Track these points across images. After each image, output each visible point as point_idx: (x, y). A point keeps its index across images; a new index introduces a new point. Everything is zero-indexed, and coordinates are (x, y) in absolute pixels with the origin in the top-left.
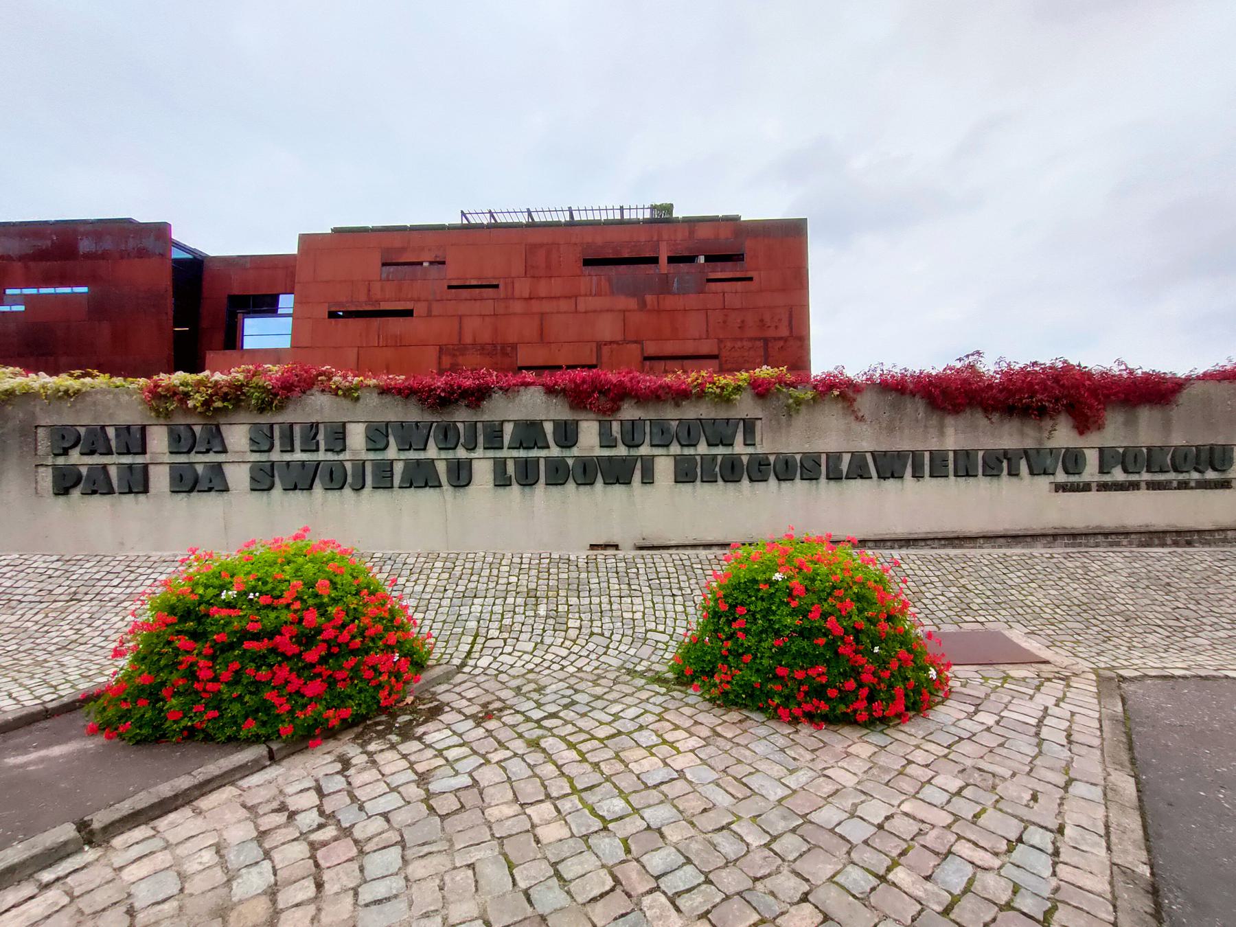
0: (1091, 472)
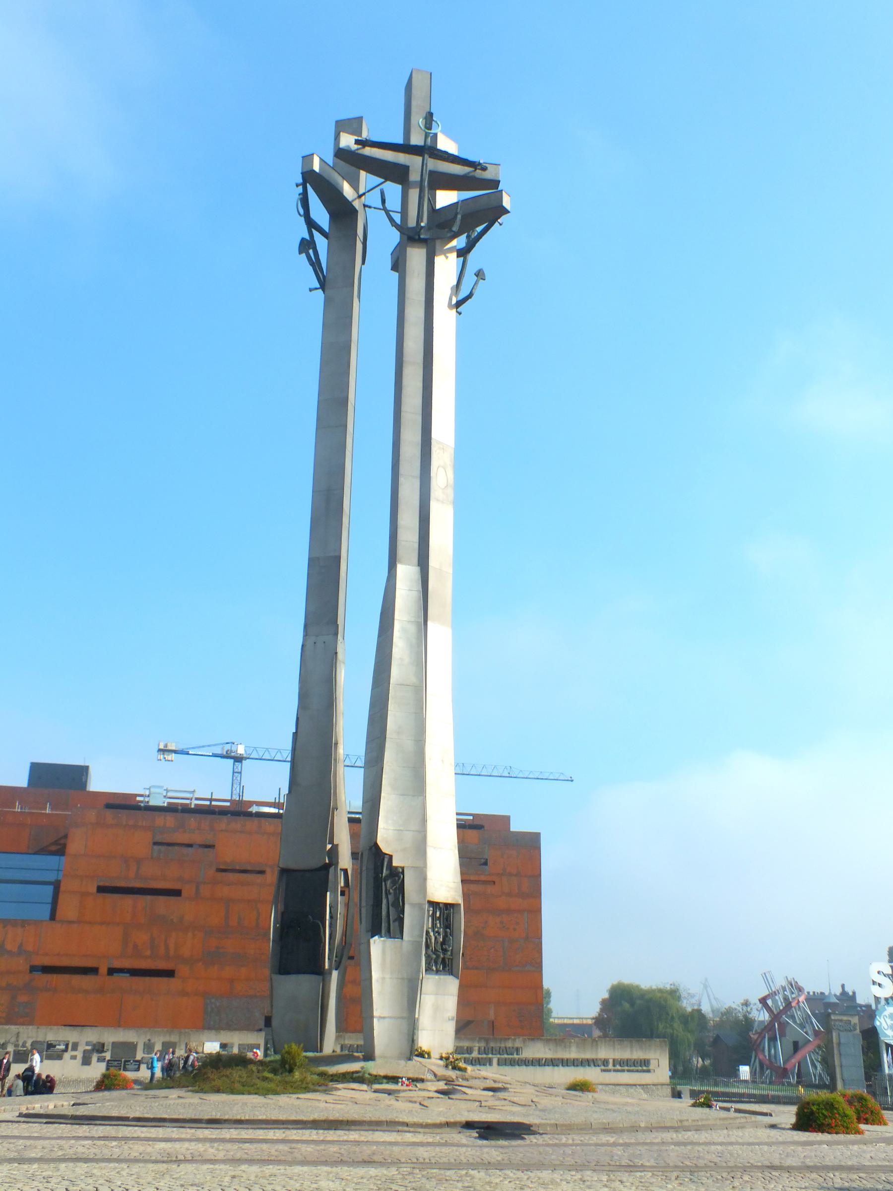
0: (610, 1067)
